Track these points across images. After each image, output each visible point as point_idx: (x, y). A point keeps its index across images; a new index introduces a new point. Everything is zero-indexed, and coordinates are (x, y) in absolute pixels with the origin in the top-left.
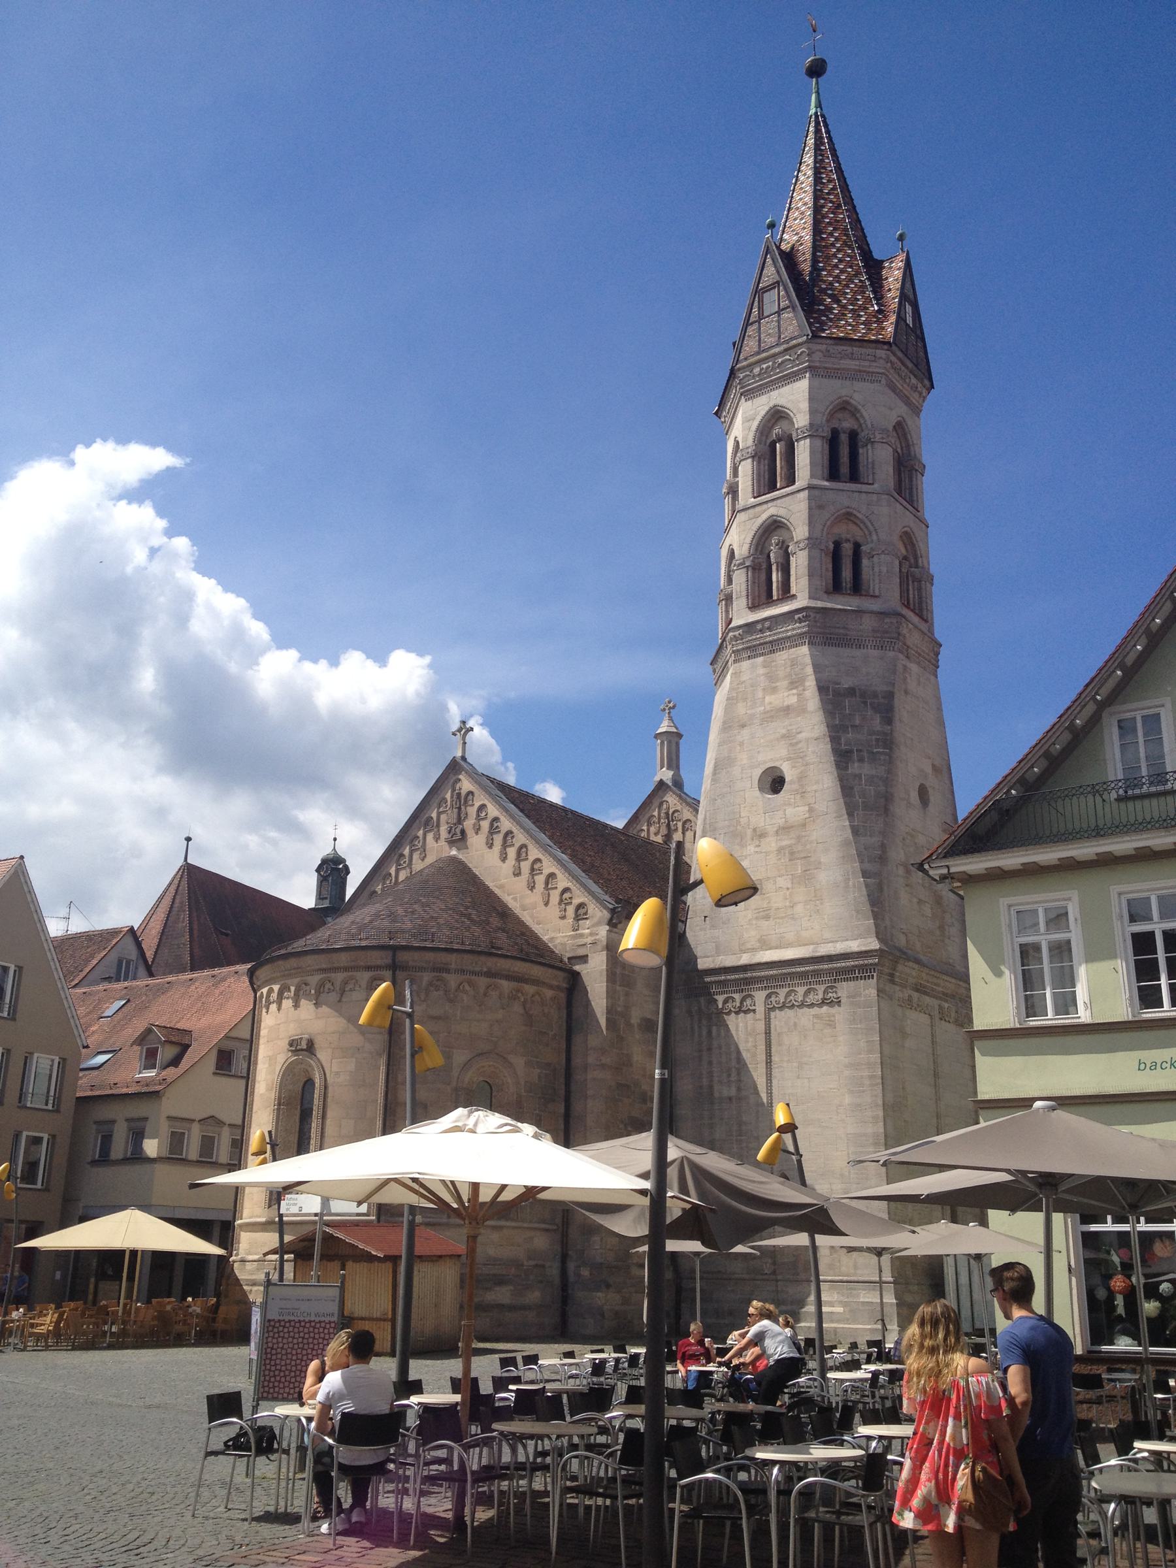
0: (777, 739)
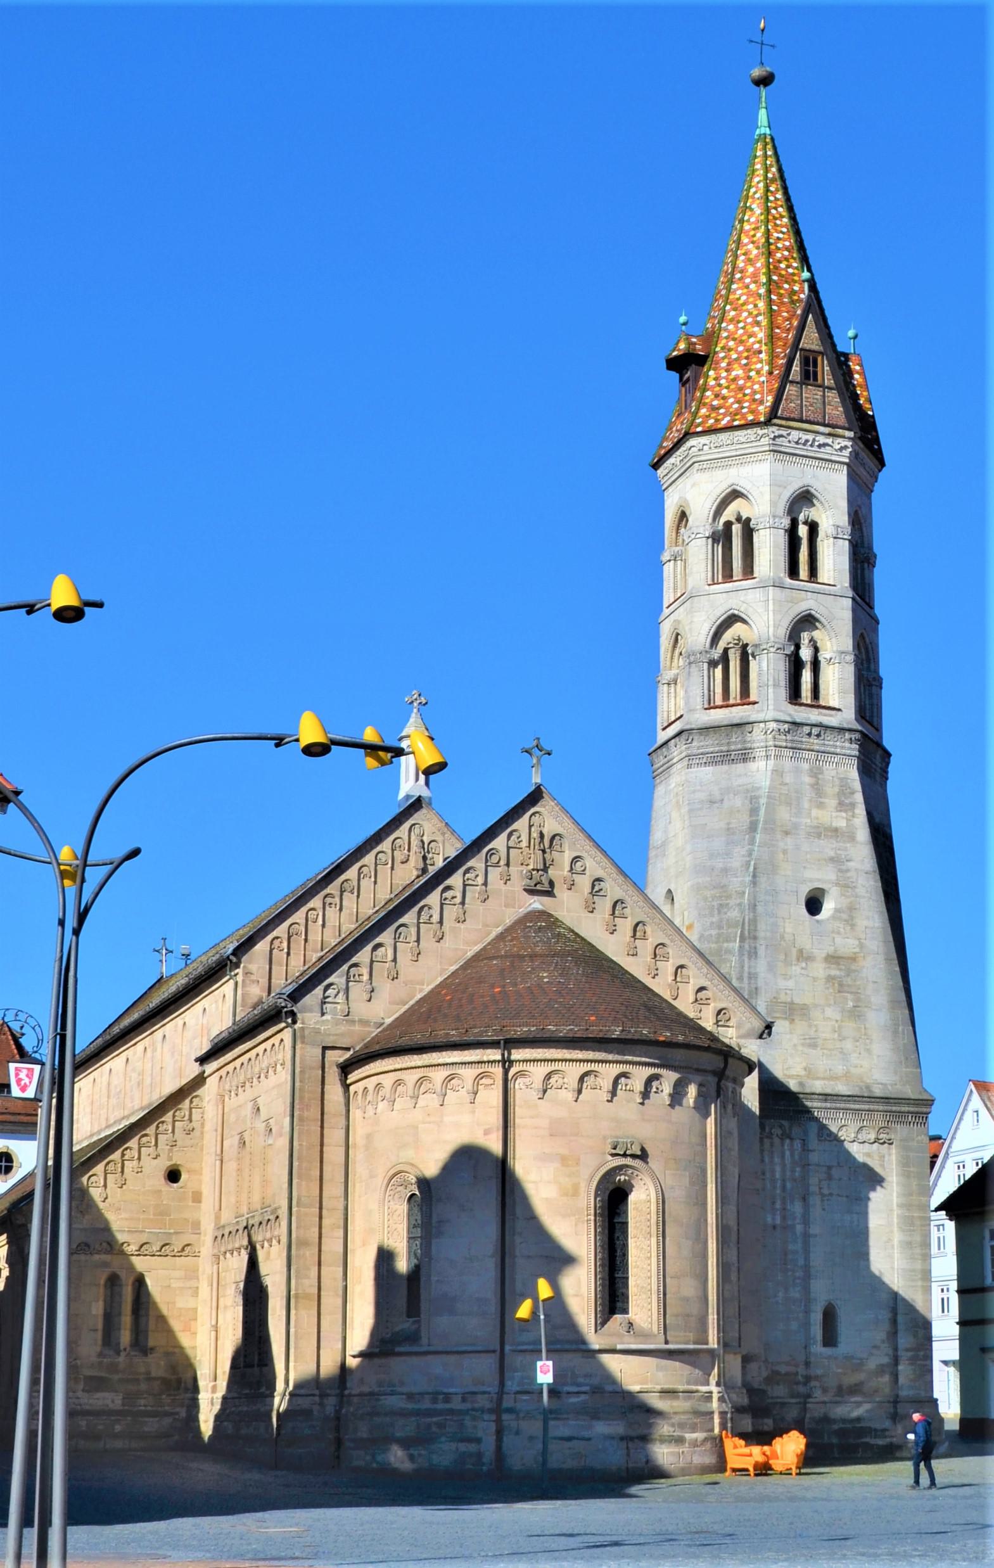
0: (825, 860)
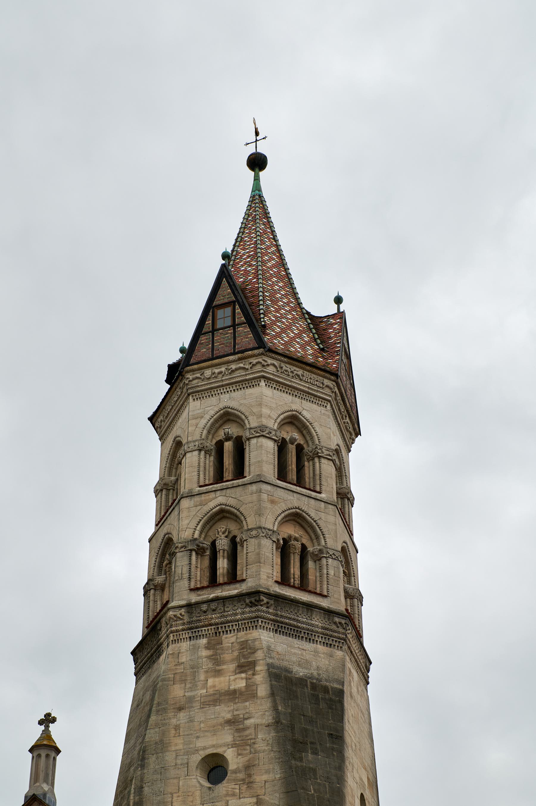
0: (221, 725)
